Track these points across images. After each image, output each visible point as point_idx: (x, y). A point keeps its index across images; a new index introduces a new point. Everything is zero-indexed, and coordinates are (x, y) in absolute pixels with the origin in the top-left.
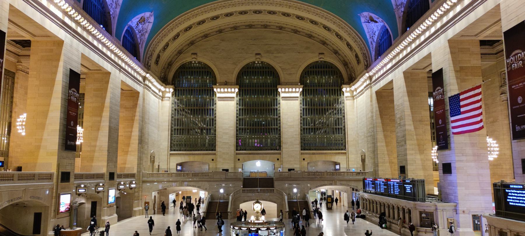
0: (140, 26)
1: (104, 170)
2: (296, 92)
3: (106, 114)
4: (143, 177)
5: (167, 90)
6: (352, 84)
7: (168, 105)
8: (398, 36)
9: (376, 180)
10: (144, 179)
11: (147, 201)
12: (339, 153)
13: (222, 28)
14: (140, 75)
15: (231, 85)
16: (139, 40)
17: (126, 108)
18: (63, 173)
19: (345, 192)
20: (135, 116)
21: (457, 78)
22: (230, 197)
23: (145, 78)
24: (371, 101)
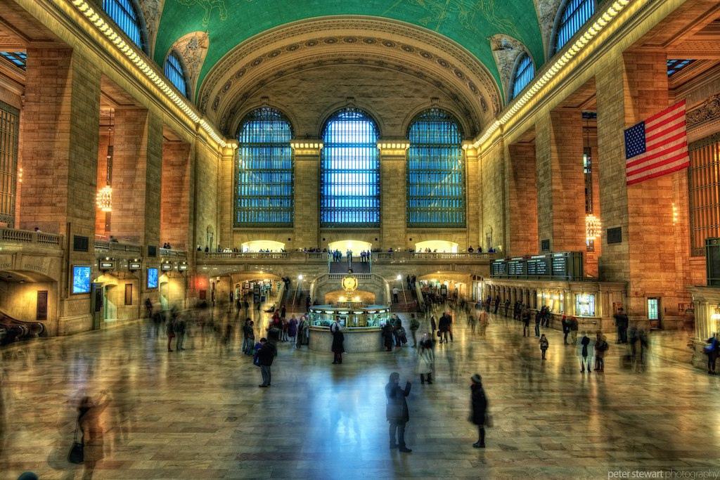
0: (191, 52)
1: (141, 243)
2: (401, 149)
3: (142, 165)
4: (197, 257)
5: (229, 145)
6: (475, 139)
7: (231, 166)
8: (544, 63)
9: (509, 259)
10: (200, 260)
11: (204, 289)
12: (457, 232)
13: (303, 63)
14: (192, 120)
15: (314, 139)
16: (190, 74)
17: (172, 165)
18: (77, 239)
19: (464, 282)
20: (185, 176)
21: (634, 107)
22: (312, 286)
23: (198, 125)
24: (503, 159)
